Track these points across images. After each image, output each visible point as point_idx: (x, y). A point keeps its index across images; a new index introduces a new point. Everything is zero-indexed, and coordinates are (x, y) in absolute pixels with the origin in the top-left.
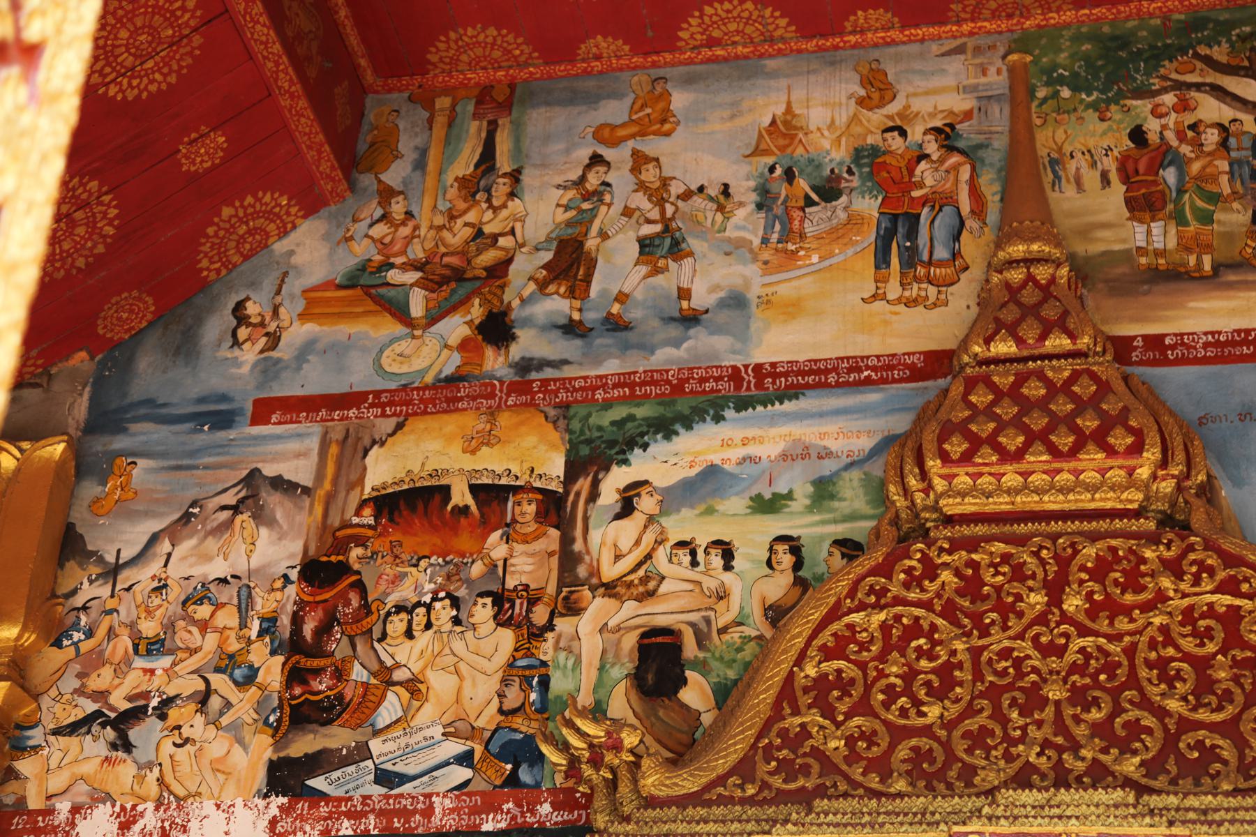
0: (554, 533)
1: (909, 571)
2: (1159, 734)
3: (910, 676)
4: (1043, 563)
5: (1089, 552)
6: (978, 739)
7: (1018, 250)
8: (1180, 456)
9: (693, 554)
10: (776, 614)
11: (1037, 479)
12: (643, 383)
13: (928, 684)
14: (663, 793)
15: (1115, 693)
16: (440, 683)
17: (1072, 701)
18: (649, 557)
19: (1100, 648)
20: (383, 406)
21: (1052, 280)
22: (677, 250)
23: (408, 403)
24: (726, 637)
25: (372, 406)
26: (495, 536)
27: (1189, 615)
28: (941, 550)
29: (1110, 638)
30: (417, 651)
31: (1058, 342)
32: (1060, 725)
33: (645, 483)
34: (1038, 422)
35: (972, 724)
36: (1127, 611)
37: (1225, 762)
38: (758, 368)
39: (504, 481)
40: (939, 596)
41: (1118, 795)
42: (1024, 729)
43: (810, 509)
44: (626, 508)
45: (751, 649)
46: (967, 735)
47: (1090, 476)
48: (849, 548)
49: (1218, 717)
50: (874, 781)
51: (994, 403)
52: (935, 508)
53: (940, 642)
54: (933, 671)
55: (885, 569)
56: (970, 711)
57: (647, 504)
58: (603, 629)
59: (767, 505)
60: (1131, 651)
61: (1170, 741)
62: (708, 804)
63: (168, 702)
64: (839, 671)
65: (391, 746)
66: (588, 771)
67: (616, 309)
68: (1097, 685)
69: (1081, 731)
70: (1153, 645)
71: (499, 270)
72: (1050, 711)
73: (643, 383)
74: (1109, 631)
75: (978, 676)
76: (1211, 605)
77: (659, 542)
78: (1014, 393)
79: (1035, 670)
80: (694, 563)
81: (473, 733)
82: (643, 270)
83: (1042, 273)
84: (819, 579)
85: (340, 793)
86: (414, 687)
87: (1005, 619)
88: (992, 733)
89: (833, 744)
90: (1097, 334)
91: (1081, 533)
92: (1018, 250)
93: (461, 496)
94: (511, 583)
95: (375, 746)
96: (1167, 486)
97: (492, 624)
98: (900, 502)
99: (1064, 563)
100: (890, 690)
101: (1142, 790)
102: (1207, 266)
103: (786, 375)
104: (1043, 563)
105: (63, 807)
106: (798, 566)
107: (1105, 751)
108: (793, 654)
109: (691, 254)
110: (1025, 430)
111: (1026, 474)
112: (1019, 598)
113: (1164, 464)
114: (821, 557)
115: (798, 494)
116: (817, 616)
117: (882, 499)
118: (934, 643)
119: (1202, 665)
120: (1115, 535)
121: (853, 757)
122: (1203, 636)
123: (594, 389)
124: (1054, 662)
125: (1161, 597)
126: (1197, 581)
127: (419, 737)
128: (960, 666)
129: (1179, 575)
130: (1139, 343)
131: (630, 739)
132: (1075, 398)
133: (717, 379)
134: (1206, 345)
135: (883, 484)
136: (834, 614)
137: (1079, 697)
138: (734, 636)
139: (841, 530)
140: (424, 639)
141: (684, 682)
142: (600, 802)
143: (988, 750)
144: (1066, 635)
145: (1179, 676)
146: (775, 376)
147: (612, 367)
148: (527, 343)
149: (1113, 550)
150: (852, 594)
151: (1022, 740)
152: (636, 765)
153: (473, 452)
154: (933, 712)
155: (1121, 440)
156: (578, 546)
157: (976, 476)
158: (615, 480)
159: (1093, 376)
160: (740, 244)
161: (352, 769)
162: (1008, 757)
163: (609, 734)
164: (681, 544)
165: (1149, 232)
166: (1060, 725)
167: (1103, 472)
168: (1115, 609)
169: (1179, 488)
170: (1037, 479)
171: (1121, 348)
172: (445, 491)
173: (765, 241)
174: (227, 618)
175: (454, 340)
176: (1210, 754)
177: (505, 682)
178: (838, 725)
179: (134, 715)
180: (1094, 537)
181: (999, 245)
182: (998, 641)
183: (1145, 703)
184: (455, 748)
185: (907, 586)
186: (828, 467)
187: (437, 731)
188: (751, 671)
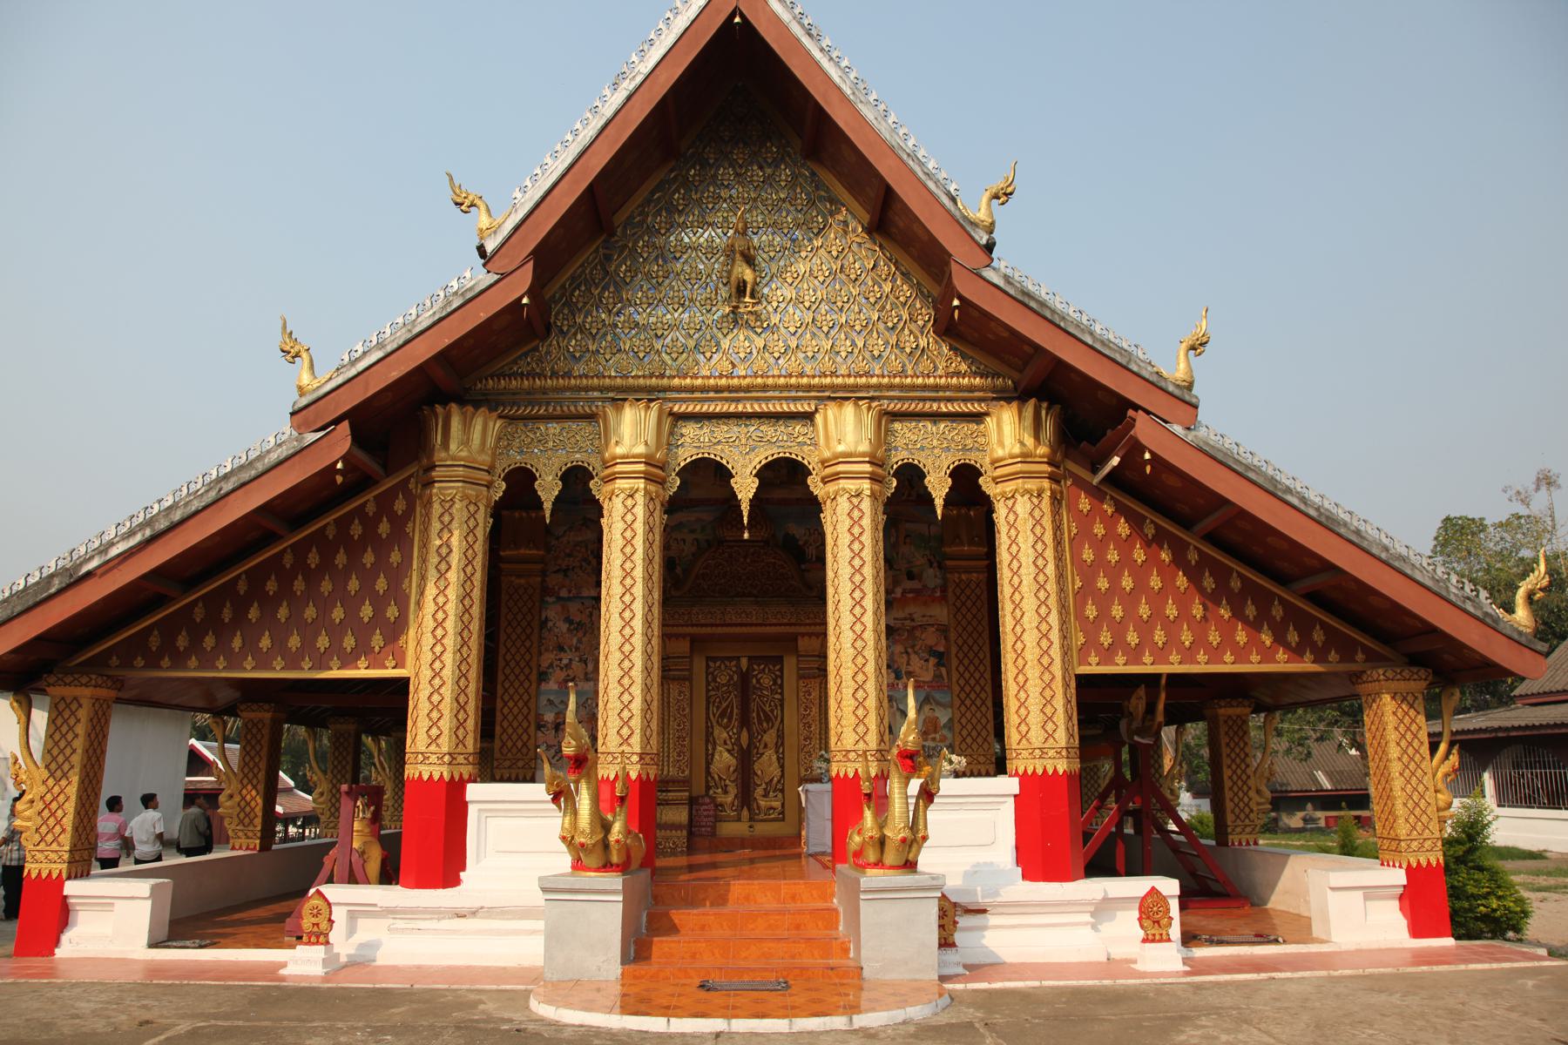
5: (752, 550)
59: (692, 531)
63: (574, 567)
105: (556, 588)
154: (723, 581)
155: (759, 527)
174: (583, 550)
179: (568, 569)
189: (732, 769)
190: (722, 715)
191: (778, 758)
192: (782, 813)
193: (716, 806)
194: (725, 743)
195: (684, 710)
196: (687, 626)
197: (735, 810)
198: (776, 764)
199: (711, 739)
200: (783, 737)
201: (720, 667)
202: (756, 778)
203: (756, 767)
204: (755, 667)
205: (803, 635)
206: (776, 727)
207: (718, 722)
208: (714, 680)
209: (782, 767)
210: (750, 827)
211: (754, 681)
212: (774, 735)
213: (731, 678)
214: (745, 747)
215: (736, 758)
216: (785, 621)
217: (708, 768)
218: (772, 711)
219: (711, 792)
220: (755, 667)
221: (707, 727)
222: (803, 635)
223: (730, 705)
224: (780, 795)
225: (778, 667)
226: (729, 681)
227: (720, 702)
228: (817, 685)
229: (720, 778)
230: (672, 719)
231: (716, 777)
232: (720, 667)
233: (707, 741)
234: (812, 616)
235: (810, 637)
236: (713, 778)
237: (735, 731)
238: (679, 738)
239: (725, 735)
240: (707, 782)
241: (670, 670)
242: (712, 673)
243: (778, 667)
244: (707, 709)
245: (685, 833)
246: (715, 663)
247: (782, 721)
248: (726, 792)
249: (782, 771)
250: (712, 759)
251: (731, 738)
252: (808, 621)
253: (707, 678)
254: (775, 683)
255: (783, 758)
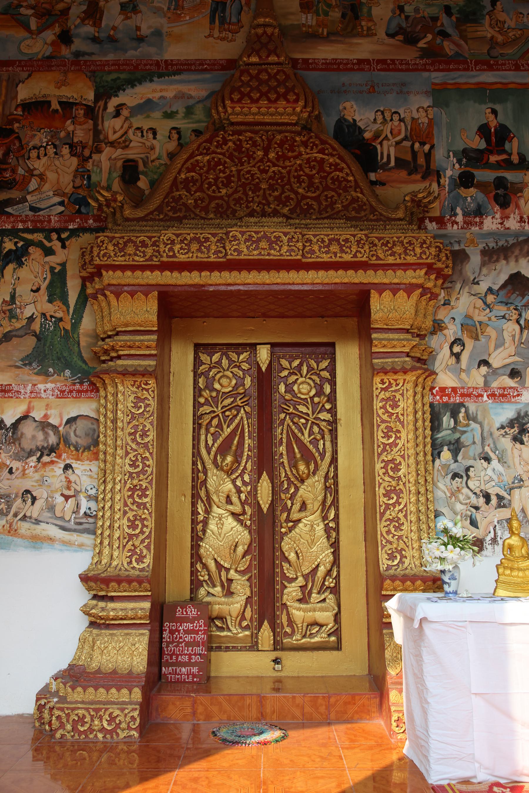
0: (91, 122)
1: (218, 142)
2: (295, 200)
3: (216, 179)
4: (263, 140)
5: (279, 137)
6: (238, 201)
7: (261, 20)
8: (310, 104)
9: (142, 132)
10: (172, 156)
11: (263, 110)
12: (123, 65)
13: (222, 182)
14: (131, 216)
15: (283, 186)
16: (51, 176)
17: (269, 189)
18: (126, 133)
19: (279, 171)
20: (23, 67)
21: (272, 34)
22: (135, 10)
23: (32, 66)
24: (154, 164)
25: (18, 66)
26: (69, 122)
27: (308, 161)
28: (229, 134)
29: (283, 168)
30: (42, 164)
31: (273, 59)
32: (265, 197)
33: (124, 104)
34: (264, 89)
35: (236, 196)
36: (289, 158)
37: (314, 209)
38: (166, 61)
39: (71, 101)
40: (227, 151)
41: (281, 219)
42: (253, 198)
43: (184, 118)
44: (117, 114)
45: (162, 168)
46: (234, 199)
47: (281, 110)
48: (197, 133)
49: (314, 195)
50: (203, 214)
51: (250, 81)
52: (228, 119)
53: (227, 167)
54: (224, 177)
55: (209, 141)
56: (236, 192)
57: (125, 112)
58: (110, 159)
59: (169, 115)
60: (289, 172)
61: (298, 203)
62: (147, 221)
64: (193, 177)
65: (34, 198)
66: (105, 209)
67: (112, 33)
68: (277, 184)
69: (271, 199)
70: (296, 170)
71: (65, 12)
72: (262, 192)
73: (123, 65)
74: (283, 165)
75: (239, 180)
76: (315, 157)
77: (130, 127)
78: (257, 77)
79: (258, 178)
80: (143, 136)
81: (64, 194)
82: (122, 17)
83: (269, 30)
84: (187, 144)
85: (17, 213)
86: (42, 177)
87: (249, 160)
88: (242, 199)
89: (190, 202)
90: (287, 57)
91: (276, 131)
92: (261, 20)
93: (55, 105)
94: (76, 140)
95: (29, 197)
96: (305, 115)
97: (69, 155)
98: (216, 116)
99: (270, 141)
100: (210, 184)
101: (288, 218)
102: (325, 33)
103: (176, 65)
104: (263, 140)
106: (179, 139)
107: (278, 205)
108: (177, 170)
109: (140, 12)
110: (260, 91)
111: (259, 108)
112: (254, 153)
113: (305, 107)
114: (188, 135)
115: (180, 112)
116: (185, 157)
117: (209, 115)
118: (225, 168)
119: (311, 177)
120: (287, 132)
121: (196, 206)
122: (312, 168)
123: (104, 65)
124: (264, 175)
125: (300, 154)
126: (312, 149)
127: (44, 195)
128: (233, 176)
129: (306, 147)
130: (300, 61)
131: (120, 198)
132: (277, 80)
133: (151, 65)
134: (323, 64)
135: (210, 110)
136: (191, 156)
137: (272, 188)
138: (157, 163)
139: (195, 126)
140: (44, 160)
141: (139, 179)
142: (110, 220)
143: (241, 204)
144: (269, 166)
145: (303, 181)
146: (172, 65)
147: (111, 57)
148: (78, 45)
149: (286, 137)
150: (198, 149)
151: (252, 201)
152: (122, 207)
153: (59, 88)
156: (100, 127)
157: (242, 108)
158: (114, 102)
159: (284, 72)
160: (159, 9)
161: (21, 205)
162: (247, 207)
163: (112, 196)
164: (138, 129)
165: (307, 18)
166: (265, 197)
167: (285, 108)
168: (285, 158)
169: (309, 116)
170: (263, 110)
171: (294, 62)
172: (49, 103)
173: (169, 8)
175: (49, 41)
176: (310, 207)
177: (75, 177)
178: (192, 195)
180: (280, 132)
181: (255, 18)
182: (246, 168)
183: (292, 190)
184: (57, 199)
185: (217, 147)
186: (191, 102)
187: (51, 193)
188: (162, 176)
189: (241, 550)
190: (223, 450)
191: (327, 530)
192: (337, 632)
193: (212, 619)
194: (229, 500)
195: (144, 434)
196: (152, 268)
197: (247, 628)
198: (324, 540)
199: (203, 494)
200: (337, 492)
201: (219, 362)
202: (286, 565)
203: (285, 546)
204: (285, 363)
205: (381, 288)
206: (322, 472)
207: (215, 462)
208: (209, 387)
209: (335, 546)
210: (276, 661)
211: (282, 388)
212: (320, 486)
213: (241, 382)
214: (265, 508)
215: (249, 529)
216: (347, 258)
217: (195, 547)
218: (314, 443)
219: (202, 592)
220: (285, 363)
221: (195, 471)
222: (381, 288)
223: (237, 430)
224: (331, 598)
225: (324, 364)
226: (236, 387)
227: (219, 426)
228: (410, 386)
229: (219, 566)
230: (119, 452)
231: (212, 565)
232: (219, 362)
233: (195, 497)
234: (398, 249)
235: (394, 292)
236: (205, 566)
237: (247, 478)
238: (133, 489)
239: (228, 486)
240: (194, 573)
241: (119, 357)
242: (205, 374)
243: (324, 364)
244: (196, 438)
245: (137, 694)
246: (211, 356)
247: (334, 460)
248: (229, 593)
249: (336, 554)
250: (204, 531)
251: (239, 491)
252: (391, 260)
253: (196, 382)
254: (320, 393)
255: (337, 529)
